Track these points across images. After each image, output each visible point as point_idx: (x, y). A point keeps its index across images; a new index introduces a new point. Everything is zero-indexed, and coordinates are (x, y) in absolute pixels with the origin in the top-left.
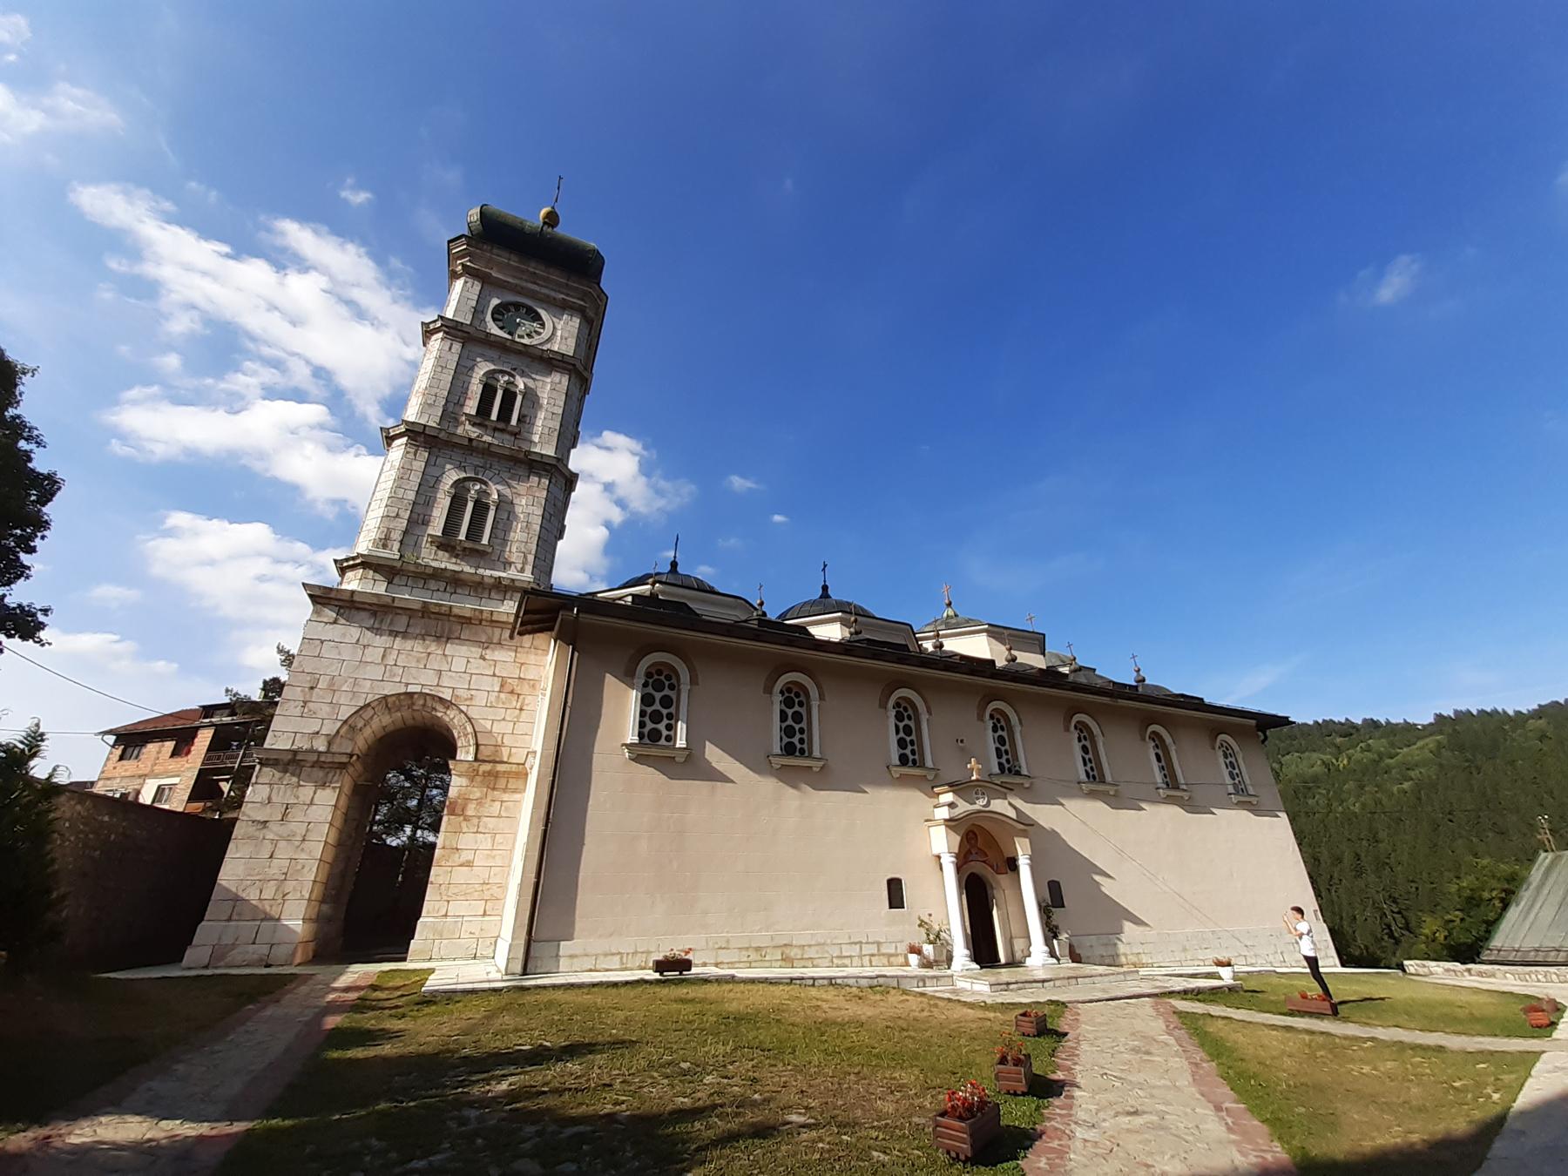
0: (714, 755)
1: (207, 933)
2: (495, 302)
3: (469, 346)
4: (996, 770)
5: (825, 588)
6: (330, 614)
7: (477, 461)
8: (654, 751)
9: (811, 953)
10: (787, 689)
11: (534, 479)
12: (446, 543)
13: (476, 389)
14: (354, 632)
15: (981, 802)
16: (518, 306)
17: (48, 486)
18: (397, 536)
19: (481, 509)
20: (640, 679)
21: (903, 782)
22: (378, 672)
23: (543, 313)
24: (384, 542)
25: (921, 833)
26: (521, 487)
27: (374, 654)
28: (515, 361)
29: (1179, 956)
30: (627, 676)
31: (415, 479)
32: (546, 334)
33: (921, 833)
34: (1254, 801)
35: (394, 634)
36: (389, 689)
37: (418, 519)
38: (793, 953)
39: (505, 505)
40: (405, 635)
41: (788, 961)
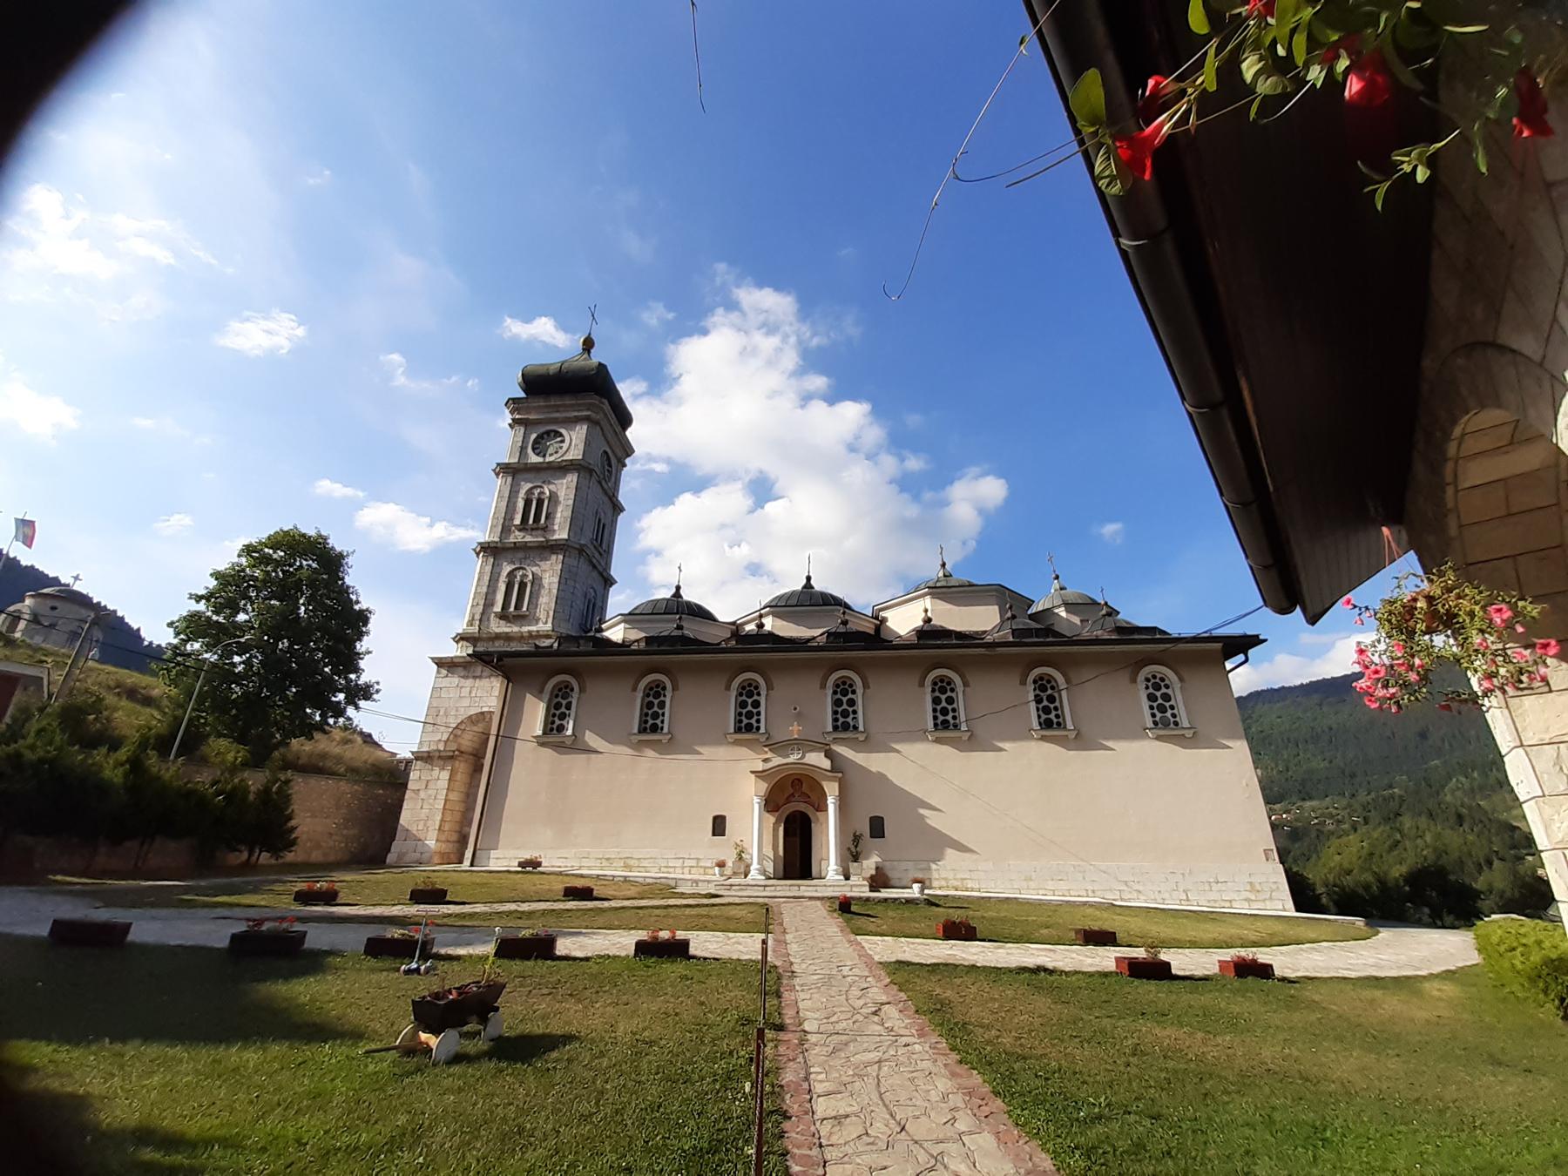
0: (591, 739)
1: (396, 847)
2: (534, 436)
3: (518, 476)
4: (830, 728)
5: (809, 578)
6: (444, 672)
7: (520, 555)
8: (551, 739)
9: (645, 863)
10: (649, 688)
11: (554, 557)
12: (503, 616)
13: (521, 504)
14: (455, 680)
15: (793, 758)
16: (548, 433)
17: (363, 617)
18: (477, 617)
19: (523, 585)
20: (546, 696)
21: (737, 743)
22: (466, 703)
23: (563, 431)
24: (471, 623)
25: (736, 781)
26: (545, 565)
27: (465, 692)
28: (543, 475)
29: (1025, 884)
30: (539, 694)
31: (487, 578)
32: (565, 446)
33: (736, 781)
34: (1189, 734)
35: (475, 678)
36: (473, 711)
37: (489, 604)
38: (632, 862)
39: (537, 580)
40: (480, 677)
41: (627, 867)
